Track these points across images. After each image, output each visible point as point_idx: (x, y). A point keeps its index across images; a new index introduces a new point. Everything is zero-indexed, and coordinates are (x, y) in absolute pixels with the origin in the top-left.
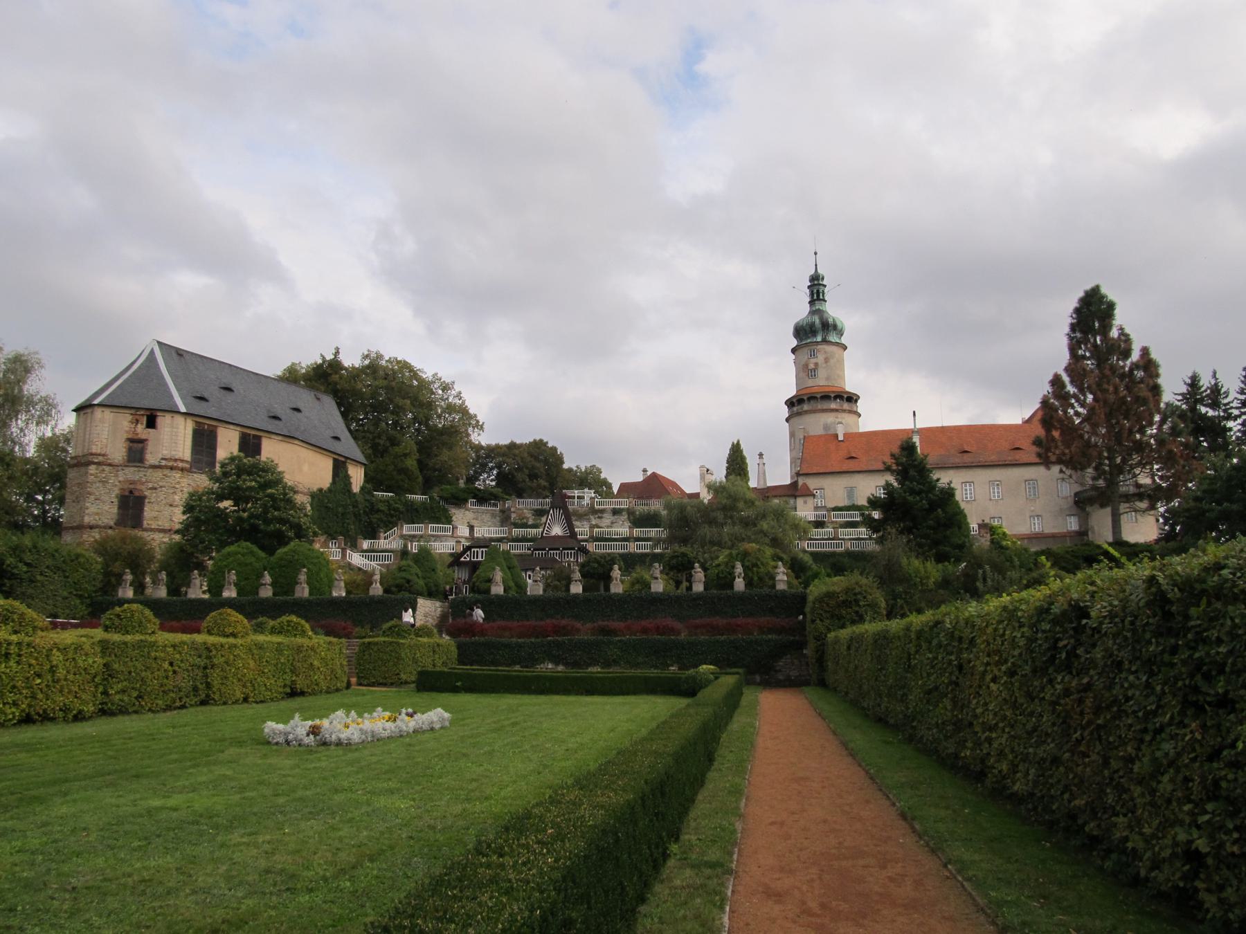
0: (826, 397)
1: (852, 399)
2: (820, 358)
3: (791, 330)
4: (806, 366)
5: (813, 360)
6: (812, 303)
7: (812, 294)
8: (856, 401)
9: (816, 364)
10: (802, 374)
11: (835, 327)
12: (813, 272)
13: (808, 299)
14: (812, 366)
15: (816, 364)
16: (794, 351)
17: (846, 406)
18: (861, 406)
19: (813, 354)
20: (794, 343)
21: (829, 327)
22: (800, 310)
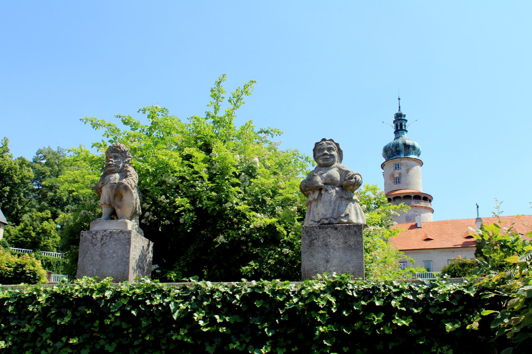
0: (407, 197)
1: (427, 198)
2: (403, 170)
3: (381, 151)
4: (393, 175)
5: (397, 171)
6: (396, 132)
7: (397, 126)
8: (430, 201)
9: (400, 174)
10: (391, 182)
11: (414, 147)
12: (397, 111)
13: (394, 130)
14: (397, 175)
15: (400, 174)
16: (383, 166)
17: (423, 204)
18: (433, 205)
19: (397, 167)
20: (384, 160)
21: (408, 148)
22: (389, 138)
